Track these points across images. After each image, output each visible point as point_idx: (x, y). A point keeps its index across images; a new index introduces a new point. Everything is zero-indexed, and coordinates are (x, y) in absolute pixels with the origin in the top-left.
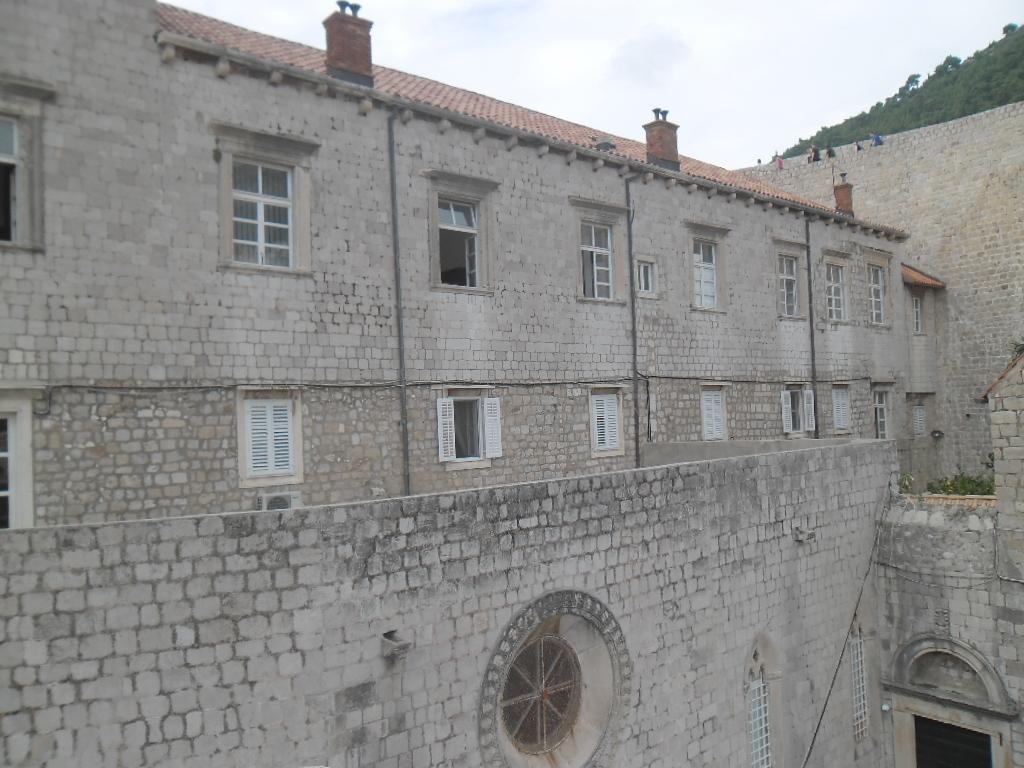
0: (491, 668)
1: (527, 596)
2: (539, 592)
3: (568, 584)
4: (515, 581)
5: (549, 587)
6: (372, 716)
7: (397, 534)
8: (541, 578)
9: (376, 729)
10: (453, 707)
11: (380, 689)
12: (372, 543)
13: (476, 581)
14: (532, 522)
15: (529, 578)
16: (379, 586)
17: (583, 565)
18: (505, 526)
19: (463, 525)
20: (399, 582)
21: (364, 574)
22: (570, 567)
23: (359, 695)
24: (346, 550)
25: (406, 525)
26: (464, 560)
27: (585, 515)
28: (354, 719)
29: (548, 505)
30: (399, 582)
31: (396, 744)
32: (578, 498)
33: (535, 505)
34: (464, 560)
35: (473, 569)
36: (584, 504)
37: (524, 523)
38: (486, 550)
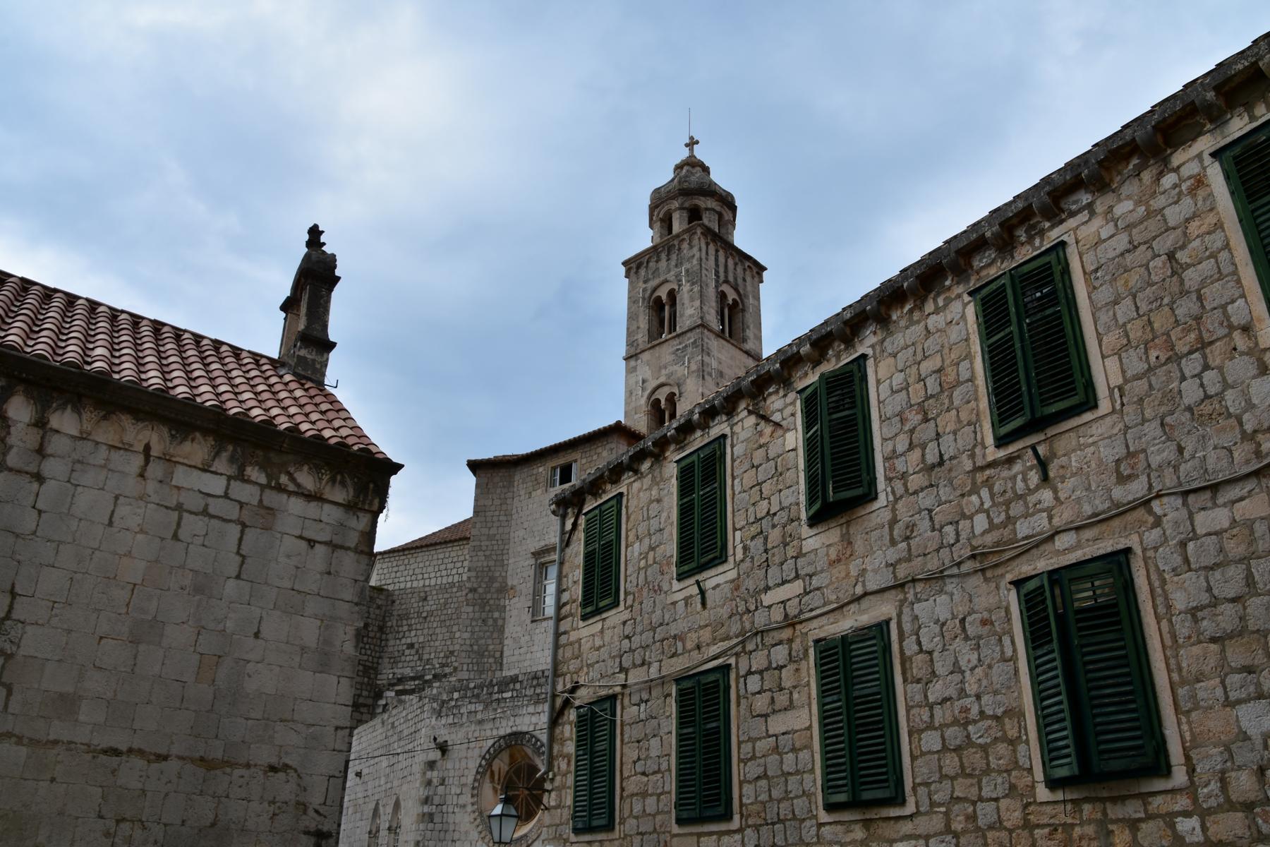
0: (480, 765)
1: (502, 732)
2: (509, 731)
3: (525, 729)
4: (497, 724)
5: (514, 729)
6: (434, 775)
7: (452, 699)
8: (511, 724)
9: (435, 781)
10: (463, 780)
11: (439, 764)
12: (443, 702)
13: (480, 722)
14: (509, 694)
15: (504, 723)
16: (443, 721)
17: (534, 719)
18: (496, 696)
19: (478, 696)
20: (450, 720)
21: (439, 715)
22: (527, 719)
23: (431, 765)
24: (435, 705)
25: (456, 695)
26: (476, 712)
27: (538, 691)
28: (429, 774)
29: (518, 686)
30: (450, 720)
31: (441, 789)
32: (535, 682)
33: (511, 686)
34: (476, 712)
35: (479, 716)
36: (539, 685)
37: (505, 695)
38: (486, 708)
